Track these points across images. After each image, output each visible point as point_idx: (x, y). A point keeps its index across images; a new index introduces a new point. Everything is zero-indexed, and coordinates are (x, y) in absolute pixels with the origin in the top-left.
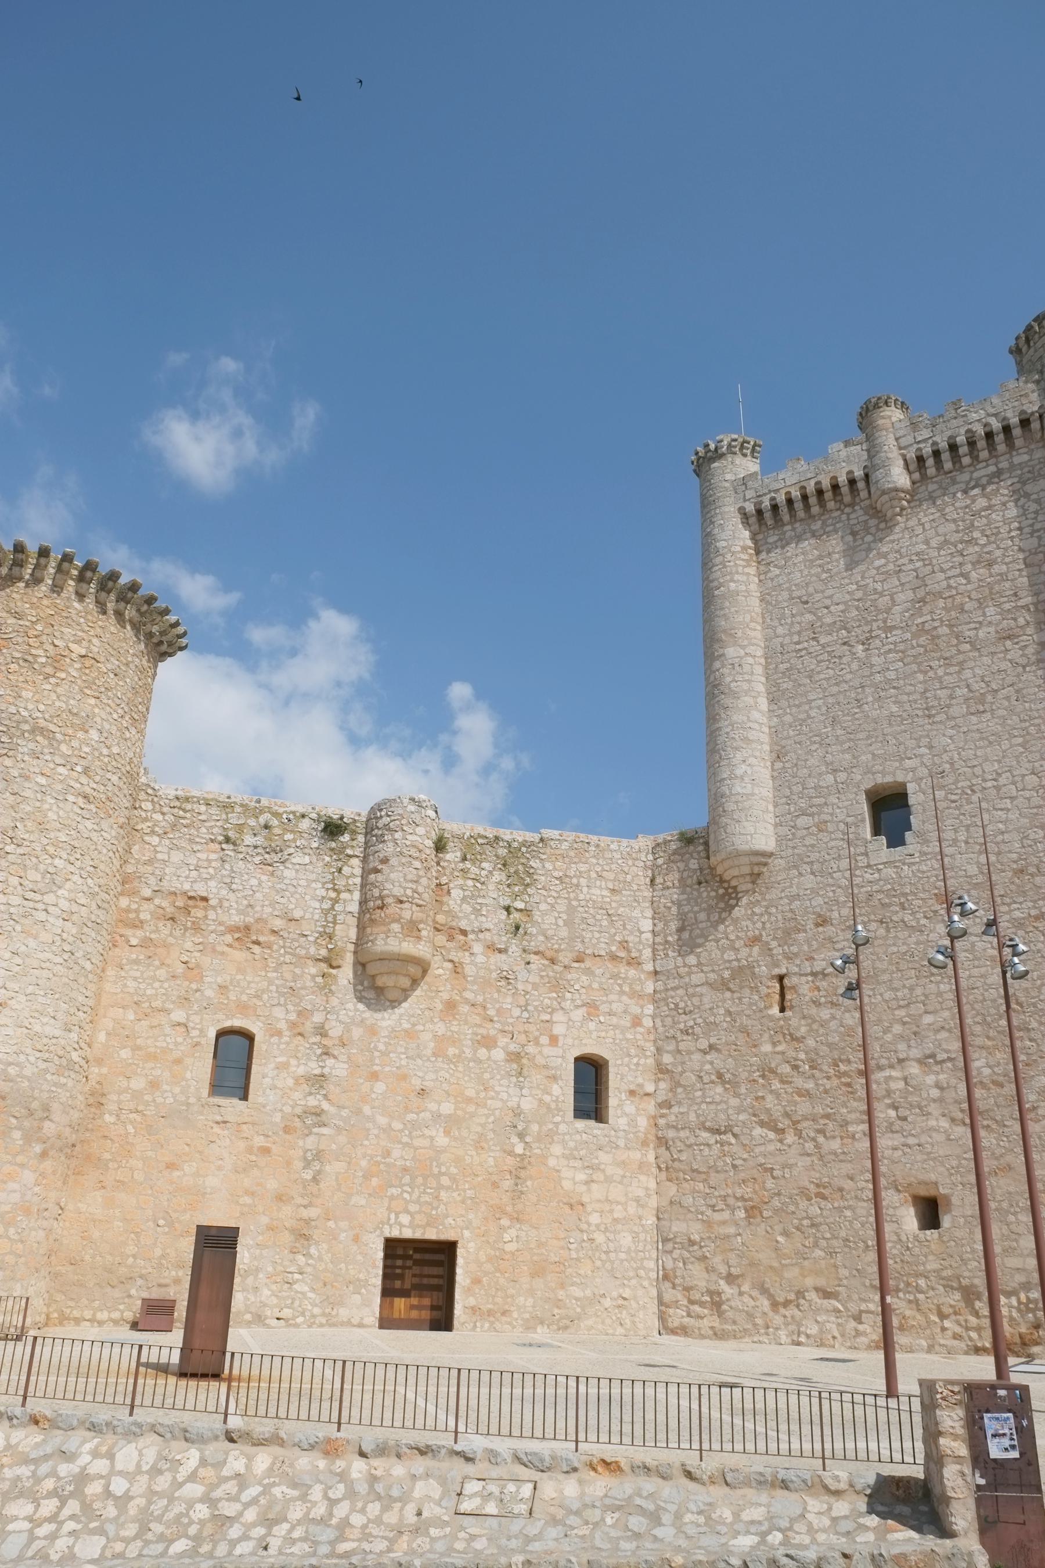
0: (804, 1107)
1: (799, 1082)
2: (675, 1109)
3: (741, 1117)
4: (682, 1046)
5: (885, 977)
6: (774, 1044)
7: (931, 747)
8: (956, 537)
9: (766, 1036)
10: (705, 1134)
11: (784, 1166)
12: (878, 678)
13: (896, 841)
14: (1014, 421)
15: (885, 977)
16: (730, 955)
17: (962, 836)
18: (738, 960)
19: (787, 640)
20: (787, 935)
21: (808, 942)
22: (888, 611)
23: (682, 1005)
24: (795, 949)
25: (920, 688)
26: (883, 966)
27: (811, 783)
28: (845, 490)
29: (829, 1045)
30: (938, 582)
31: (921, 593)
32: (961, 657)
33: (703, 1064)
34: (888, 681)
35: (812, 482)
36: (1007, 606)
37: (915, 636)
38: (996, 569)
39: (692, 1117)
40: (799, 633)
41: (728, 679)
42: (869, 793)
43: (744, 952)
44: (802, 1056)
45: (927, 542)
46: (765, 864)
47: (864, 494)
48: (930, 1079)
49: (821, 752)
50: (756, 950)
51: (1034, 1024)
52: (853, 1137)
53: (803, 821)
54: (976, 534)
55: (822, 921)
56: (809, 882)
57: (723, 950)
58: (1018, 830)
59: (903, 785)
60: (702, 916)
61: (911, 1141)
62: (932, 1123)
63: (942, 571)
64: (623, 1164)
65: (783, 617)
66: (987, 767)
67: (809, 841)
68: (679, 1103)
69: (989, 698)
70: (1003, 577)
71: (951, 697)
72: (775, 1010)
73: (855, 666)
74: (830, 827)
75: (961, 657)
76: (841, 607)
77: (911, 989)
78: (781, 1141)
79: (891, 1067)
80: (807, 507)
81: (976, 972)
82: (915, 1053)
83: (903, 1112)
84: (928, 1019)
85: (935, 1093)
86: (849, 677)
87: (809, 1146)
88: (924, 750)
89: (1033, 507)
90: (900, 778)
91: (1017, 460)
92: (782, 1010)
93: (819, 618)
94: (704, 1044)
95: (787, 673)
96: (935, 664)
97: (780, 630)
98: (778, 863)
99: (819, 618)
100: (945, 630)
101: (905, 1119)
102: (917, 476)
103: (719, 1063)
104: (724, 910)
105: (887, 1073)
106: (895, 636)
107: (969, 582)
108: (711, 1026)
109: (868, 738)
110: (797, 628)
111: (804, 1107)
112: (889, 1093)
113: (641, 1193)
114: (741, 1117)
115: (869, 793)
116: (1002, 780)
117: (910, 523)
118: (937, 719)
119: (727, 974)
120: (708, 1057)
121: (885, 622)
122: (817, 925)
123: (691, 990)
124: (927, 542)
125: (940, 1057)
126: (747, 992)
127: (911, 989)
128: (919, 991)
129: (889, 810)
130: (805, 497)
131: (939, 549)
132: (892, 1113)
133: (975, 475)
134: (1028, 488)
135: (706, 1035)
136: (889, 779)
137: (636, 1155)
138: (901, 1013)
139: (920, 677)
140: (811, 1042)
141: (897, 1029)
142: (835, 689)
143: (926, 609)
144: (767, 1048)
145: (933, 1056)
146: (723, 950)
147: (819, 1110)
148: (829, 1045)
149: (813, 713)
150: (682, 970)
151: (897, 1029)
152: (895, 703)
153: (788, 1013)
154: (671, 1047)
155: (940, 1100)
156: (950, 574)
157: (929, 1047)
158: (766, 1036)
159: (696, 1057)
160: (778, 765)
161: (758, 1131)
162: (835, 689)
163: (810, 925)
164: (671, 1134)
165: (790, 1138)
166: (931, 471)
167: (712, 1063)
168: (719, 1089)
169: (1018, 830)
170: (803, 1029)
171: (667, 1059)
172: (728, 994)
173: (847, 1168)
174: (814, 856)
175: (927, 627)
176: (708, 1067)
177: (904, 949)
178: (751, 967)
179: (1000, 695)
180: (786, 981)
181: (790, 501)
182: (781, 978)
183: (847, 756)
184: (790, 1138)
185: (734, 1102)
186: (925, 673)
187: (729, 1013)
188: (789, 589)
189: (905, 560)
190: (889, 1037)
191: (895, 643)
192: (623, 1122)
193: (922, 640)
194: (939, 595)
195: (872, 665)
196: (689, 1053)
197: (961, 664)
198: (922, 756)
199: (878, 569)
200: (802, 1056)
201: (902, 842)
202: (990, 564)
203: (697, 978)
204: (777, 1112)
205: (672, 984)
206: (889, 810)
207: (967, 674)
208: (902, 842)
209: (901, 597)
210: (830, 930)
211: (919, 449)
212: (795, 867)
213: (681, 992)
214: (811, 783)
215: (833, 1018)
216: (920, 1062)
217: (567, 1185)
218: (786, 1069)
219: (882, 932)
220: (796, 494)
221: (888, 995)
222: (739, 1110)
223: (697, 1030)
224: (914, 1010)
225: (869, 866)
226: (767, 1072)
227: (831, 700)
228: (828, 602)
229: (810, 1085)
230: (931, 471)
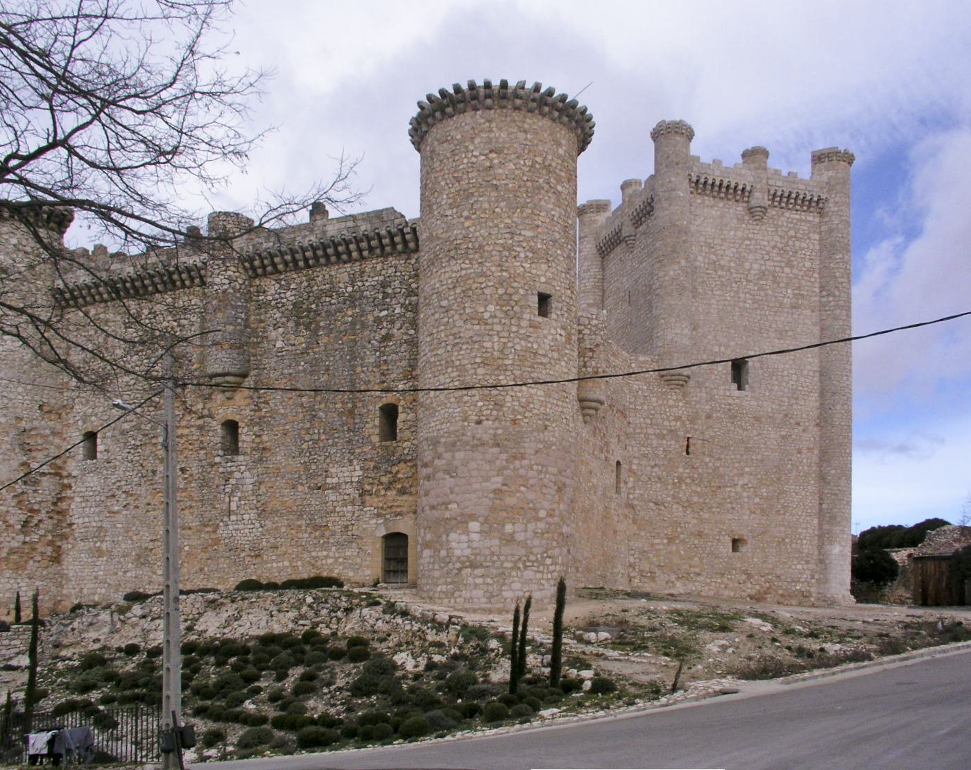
0: (695, 499)
1: (694, 488)
2: (637, 492)
3: (669, 499)
10: (652, 505)
12: (741, 304)
16: (666, 423)
22: (749, 270)
24: (696, 427)
25: (758, 317)
36: (796, 292)
48: (745, 494)
50: (679, 424)
55: (709, 417)
72: (684, 454)
74: (716, 372)
82: (741, 483)
84: (747, 469)
85: (746, 500)
89: (811, 247)
92: (688, 453)
100: (770, 292)
105: (729, 489)
106: (751, 286)
111: (695, 499)
114: (669, 499)
119: (665, 432)
125: (750, 485)
126: (673, 442)
128: (745, 457)
132: (729, 506)
138: (737, 465)
141: (735, 471)
144: (681, 470)
146: (663, 420)
151: (735, 471)
153: (691, 456)
157: (746, 481)
159: (649, 469)
161: (675, 506)
163: (703, 417)
164: (636, 502)
168: (659, 485)
171: (634, 467)
174: (707, 385)
178: (676, 430)
180: (691, 441)
182: (688, 438)
185: (666, 492)
204: (684, 499)
218: (688, 481)
222: (668, 496)
226: (681, 480)
229: (699, 489)
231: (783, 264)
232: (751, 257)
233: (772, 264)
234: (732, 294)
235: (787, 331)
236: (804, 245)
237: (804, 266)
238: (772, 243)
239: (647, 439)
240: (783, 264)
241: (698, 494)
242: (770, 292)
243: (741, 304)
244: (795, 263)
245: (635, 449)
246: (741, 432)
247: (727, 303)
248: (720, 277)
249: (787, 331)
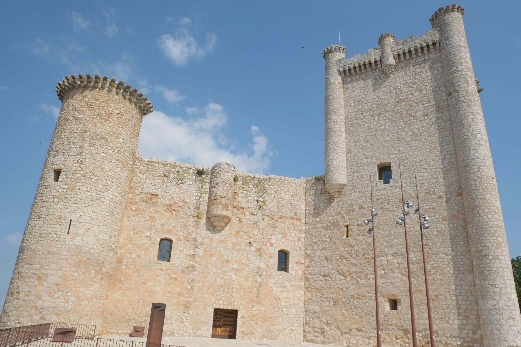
0: (353, 269)
1: (352, 261)
2: (311, 268)
3: (333, 272)
4: (314, 248)
5: (382, 227)
6: (344, 248)
7: (399, 151)
8: (409, 81)
9: (342, 245)
10: (321, 277)
11: (346, 288)
12: (382, 127)
13: (387, 182)
14: (431, 43)
15: (382, 227)
17: (409, 181)
18: (333, 220)
20: (350, 212)
21: (356, 214)
22: (386, 105)
23: (314, 234)
24: (352, 217)
25: (396, 131)
26: (381, 223)
27: (359, 161)
28: (373, 64)
29: (362, 249)
30: (403, 96)
31: (397, 100)
32: (410, 121)
33: (321, 254)
34: (386, 129)
35: (362, 62)
36: (426, 105)
37: (395, 114)
38: (423, 92)
39: (317, 271)
40: (357, 112)
41: (333, 126)
42: (378, 166)
43: (335, 217)
44: (353, 252)
45: (400, 83)
46: (343, 188)
47: (379, 66)
48: (395, 261)
49: (363, 152)
50: (339, 216)
51: (430, 244)
52: (369, 279)
53: (356, 174)
54: (417, 81)
55: (361, 208)
56: (357, 194)
57: (328, 216)
58: (427, 179)
59: (390, 163)
60: (322, 205)
61: (389, 281)
62: (396, 275)
63: (405, 92)
64: (293, 286)
65: (351, 106)
66: (418, 158)
67: (358, 181)
68: (312, 266)
69: (419, 135)
70: (425, 95)
71: (406, 135)
72: (345, 237)
73: (375, 123)
74: (365, 177)
75: (410, 121)
76: (371, 104)
77: (390, 231)
78: (346, 280)
79: (383, 256)
80: (360, 70)
81: (412, 226)
82: (391, 252)
83: (386, 271)
84: (395, 241)
85: (397, 265)
86: (373, 127)
87: (355, 282)
88: (397, 152)
89: (436, 72)
90: (389, 161)
91: (431, 56)
92: (347, 237)
93: (363, 107)
94: (321, 247)
95: (352, 125)
96: (401, 123)
97: (350, 111)
98: (347, 188)
99: (363, 107)
100: (405, 112)
101: (387, 274)
102: (397, 61)
103: (326, 254)
104: (329, 203)
105: (381, 258)
107: (414, 97)
108: (324, 241)
109: (378, 147)
110: (356, 110)
111: (353, 269)
112: (382, 265)
113: (299, 296)
114: (333, 272)
115: (378, 166)
116: (423, 163)
117: (395, 76)
118: (402, 142)
120: (322, 252)
121: (385, 109)
122: (360, 209)
123: (317, 229)
124: (400, 83)
125: (399, 254)
127: (390, 231)
128: (393, 232)
129: (385, 172)
130: (360, 67)
131: (404, 85)
132: (383, 272)
133: (417, 61)
134: (434, 66)
135: (322, 244)
136: (385, 161)
137: (298, 283)
138: (387, 239)
139: (396, 128)
140: (356, 248)
141: (385, 244)
142: (368, 131)
143: (399, 105)
144: (342, 249)
145: (397, 253)
146: (328, 216)
147: (359, 270)
148: (362, 249)
150: (315, 223)
151: (385, 244)
152: (388, 136)
153: (349, 238)
154: (310, 248)
155: (399, 268)
156: (407, 93)
157: (395, 250)
158: (342, 245)
159: (318, 251)
160: (348, 155)
161: (338, 276)
162: (368, 131)
163: (357, 209)
164: (309, 276)
165: (349, 279)
166: (402, 59)
167: (323, 254)
168: (326, 262)
169: (427, 179)
170: (354, 243)
171: (309, 252)
172: (329, 231)
173: (367, 289)
174: (359, 186)
175: (399, 111)
176: (322, 255)
177: (388, 218)
180: (349, 227)
181: (355, 68)
182: (347, 226)
183: (371, 153)
184: (349, 279)
185: (331, 266)
186: (398, 126)
187: (330, 237)
188: (354, 97)
189: (393, 89)
190: (382, 247)
191: (388, 116)
192: (293, 272)
193: (398, 115)
195: (381, 123)
196: (316, 250)
197: (410, 124)
198: (396, 154)
199: (383, 91)
200: (353, 252)
201: (389, 182)
202: (421, 91)
203: (320, 225)
204: (345, 270)
205: (311, 227)
206: (385, 172)
207: (412, 127)
208: (389, 182)
209: (391, 101)
210: (364, 211)
211: (399, 52)
212: (353, 189)
213: (314, 230)
214: (359, 161)
215: (364, 240)
216: (392, 255)
217: (275, 292)
218: (348, 256)
219: (381, 212)
220: (357, 65)
221: (382, 233)
222: (332, 269)
223: (319, 243)
224: (391, 238)
225: (377, 190)
226: (342, 257)
227: (366, 134)
228: (366, 102)
229: (356, 262)
230: (402, 59)
233: (404, 94)
239: (317, 231)
241: (354, 264)
245: (310, 239)
246: (388, 213)
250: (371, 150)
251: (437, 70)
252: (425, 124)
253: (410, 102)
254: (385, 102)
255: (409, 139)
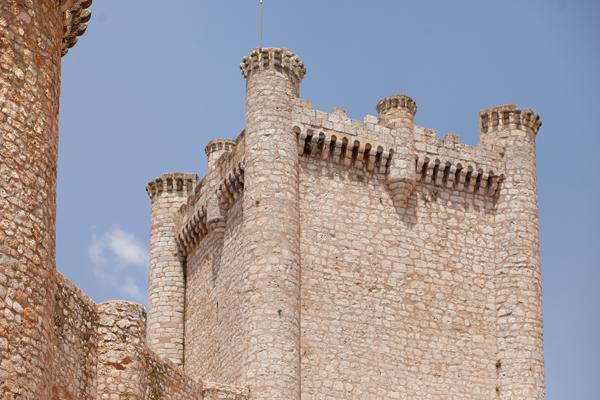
8: (435, 239)
12: (379, 322)
14: (486, 175)
19: (317, 260)
22: (389, 273)
27: (327, 383)
28: (372, 159)
30: (421, 267)
32: (430, 331)
34: (384, 327)
35: (354, 139)
36: (461, 308)
38: (457, 277)
40: (327, 259)
47: (383, 169)
63: (425, 260)
75: (430, 331)
76: (357, 253)
86: (359, 312)
89: (482, 243)
100: (421, 306)
102: (419, 176)
106: (392, 294)
107: (440, 278)
109: (368, 365)
110: (325, 254)
118: (413, 369)
121: (386, 280)
130: (344, 146)
142: (349, 318)
143: (414, 284)
149: (333, 329)
152: (388, 346)
156: (429, 265)
162: (349, 318)
166: (428, 179)
175: (413, 298)
179: (451, 368)
181: (333, 144)
186: (408, 332)
189: (403, 239)
193: (410, 307)
194: (421, 277)
195: (375, 311)
197: (430, 335)
198: (400, 392)
199: (385, 235)
211: (427, 159)
214: (327, 383)
220: (339, 141)
230: (428, 179)
231: (441, 267)
232: (393, 252)
233: (425, 265)
234: (363, 305)
235: (447, 365)
236: (470, 240)
237: (472, 270)
238: (424, 235)
240: (441, 267)
242: (421, 306)
243: (379, 322)
244: (459, 266)
247: (355, 318)
248: (344, 279)
249: (447, 365)
250: (353, 365)
251: (485, 240)
252: (454, 349)
253: (433, 288)
254: (386, 263)
255: (425, 369)
